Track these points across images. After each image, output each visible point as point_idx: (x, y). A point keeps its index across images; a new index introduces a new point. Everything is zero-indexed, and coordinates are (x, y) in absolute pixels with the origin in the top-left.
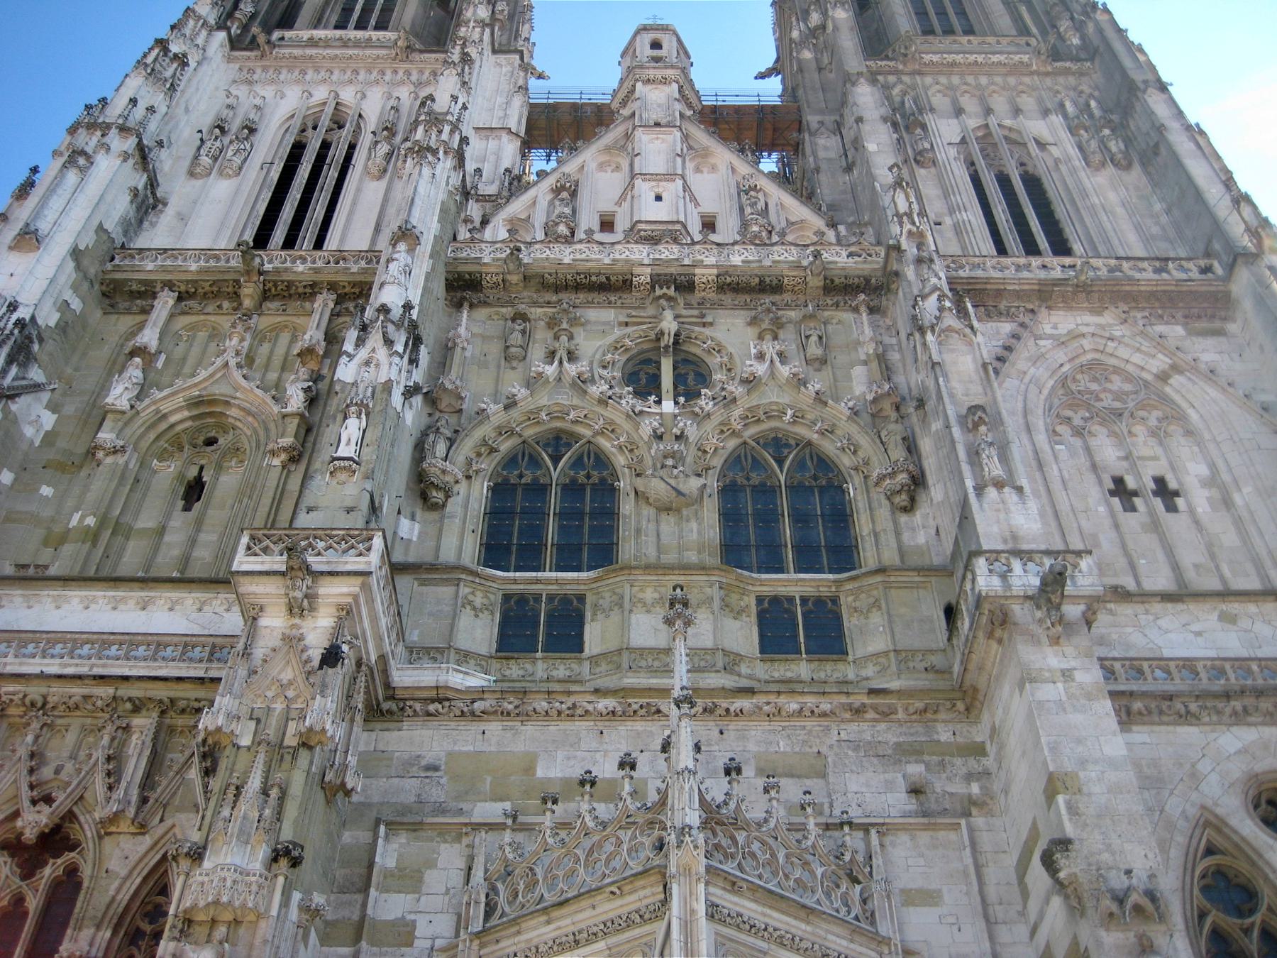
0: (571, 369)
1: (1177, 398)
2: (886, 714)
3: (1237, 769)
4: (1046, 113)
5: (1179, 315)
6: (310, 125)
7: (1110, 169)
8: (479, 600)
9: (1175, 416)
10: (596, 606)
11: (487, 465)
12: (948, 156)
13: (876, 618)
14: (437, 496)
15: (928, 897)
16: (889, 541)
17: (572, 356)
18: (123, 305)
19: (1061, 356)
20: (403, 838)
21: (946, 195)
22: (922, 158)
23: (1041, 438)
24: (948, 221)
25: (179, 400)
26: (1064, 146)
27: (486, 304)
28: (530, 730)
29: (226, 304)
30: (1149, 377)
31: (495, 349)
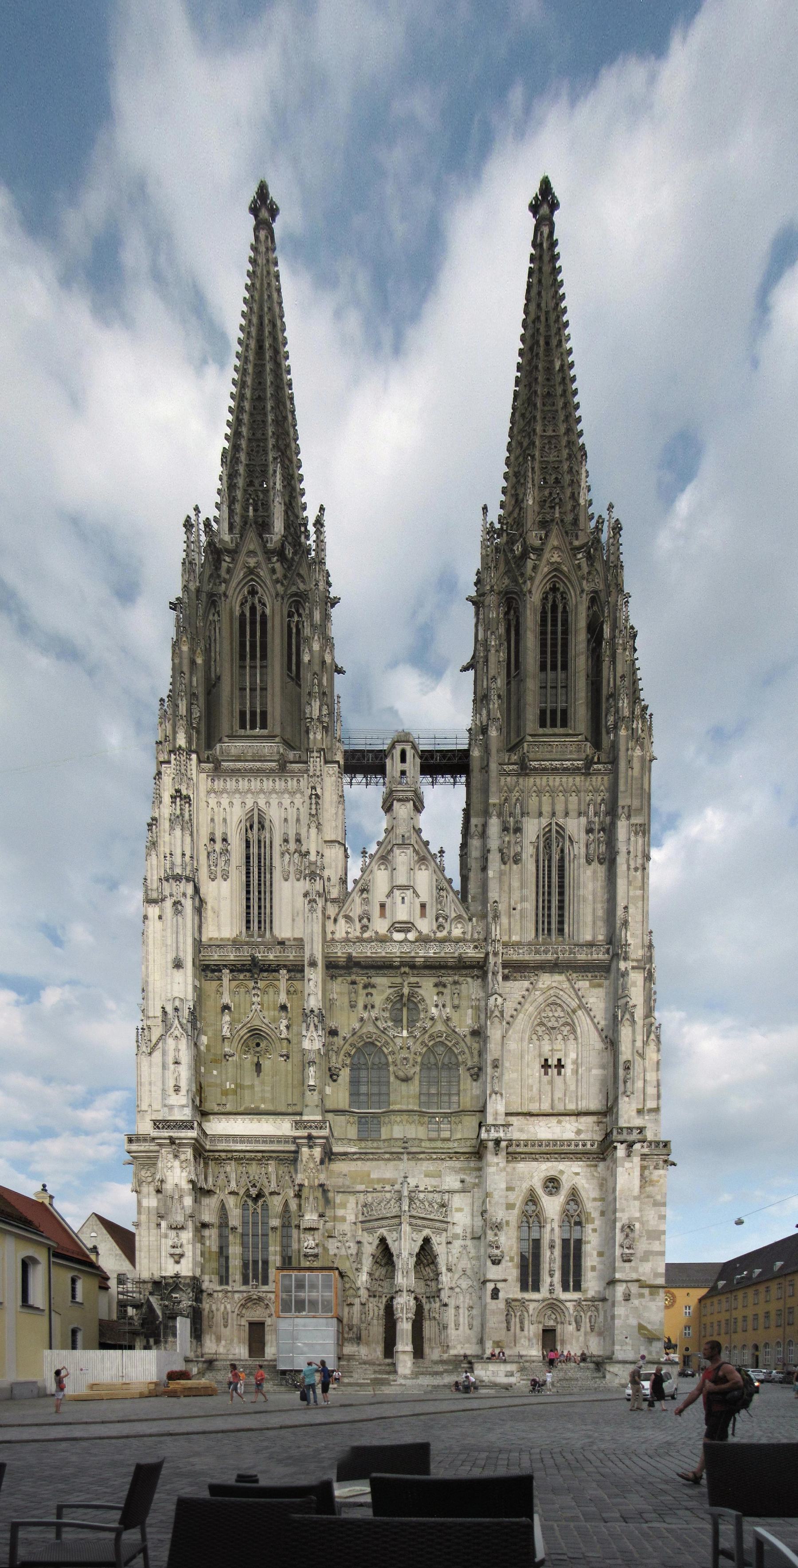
0: (374, 1014)
1: (576, 1021)
2: (458, 1159)
3: (543, 1175)
4: (580, 814)
5: (590, 975)
6: (248, 825)
7: (595, 864)
8: (351, 1120)
9: (574, 1031)
10: (384, 1123)
11: (348, 1062)
12: (528, 853)
13: (460, 1126)
14: (335, 1077)
15: (459, 1210)
16: (469, 1094)
17: (373, 1007)
18: (210, 975)
19: (541, 999)
20: (340, 1195)
21: (522, 887)
22: (517, 860)
23: (525, 1043)
24: (519, 907)
25: (245, 1030)
26: (580, 849)
27: (341, 976)
28: (369, 1163)
29: (248, 974)
30: (569, 1010)
31: (346, 1000)
